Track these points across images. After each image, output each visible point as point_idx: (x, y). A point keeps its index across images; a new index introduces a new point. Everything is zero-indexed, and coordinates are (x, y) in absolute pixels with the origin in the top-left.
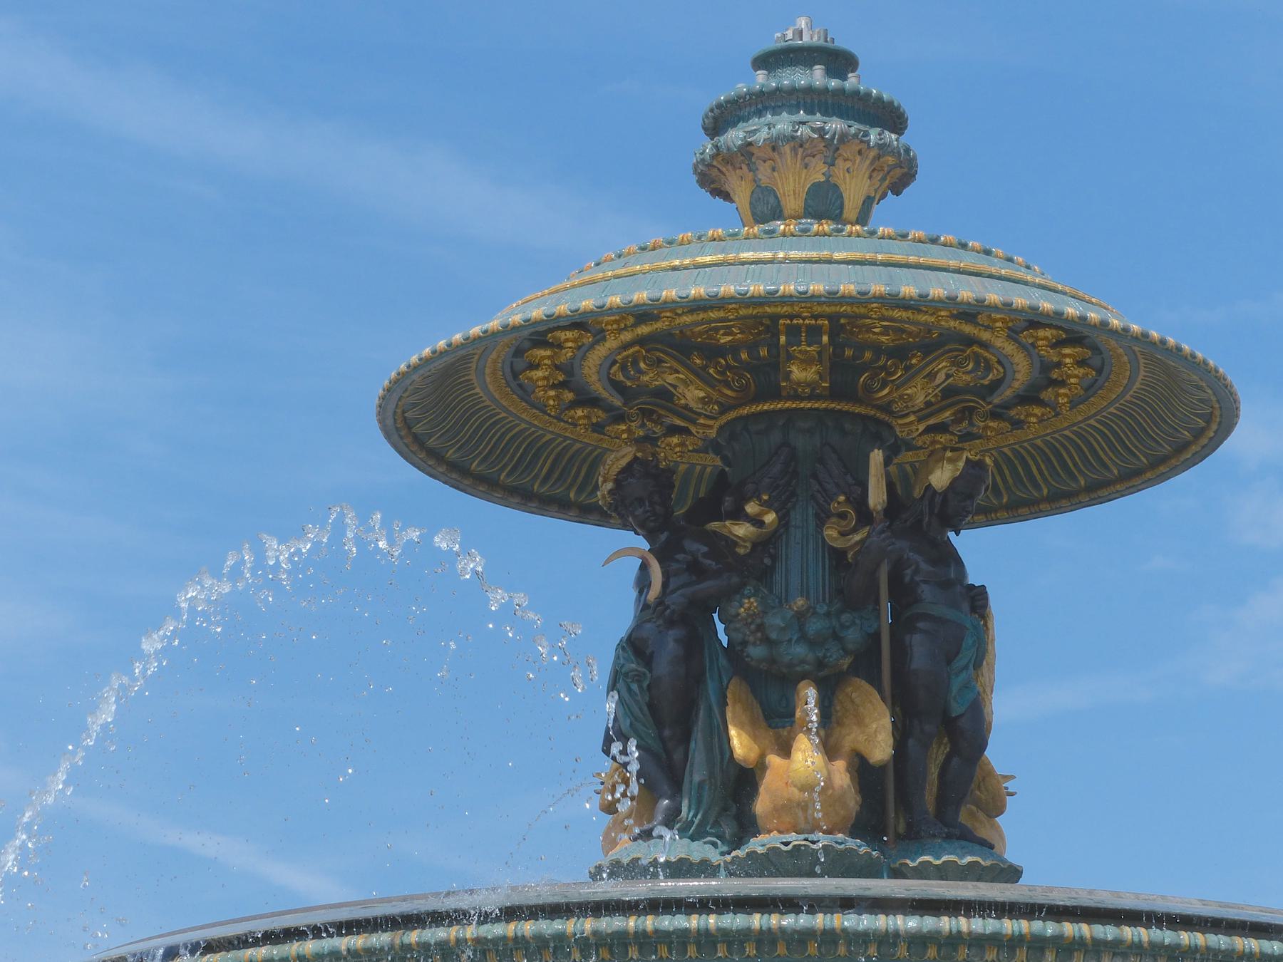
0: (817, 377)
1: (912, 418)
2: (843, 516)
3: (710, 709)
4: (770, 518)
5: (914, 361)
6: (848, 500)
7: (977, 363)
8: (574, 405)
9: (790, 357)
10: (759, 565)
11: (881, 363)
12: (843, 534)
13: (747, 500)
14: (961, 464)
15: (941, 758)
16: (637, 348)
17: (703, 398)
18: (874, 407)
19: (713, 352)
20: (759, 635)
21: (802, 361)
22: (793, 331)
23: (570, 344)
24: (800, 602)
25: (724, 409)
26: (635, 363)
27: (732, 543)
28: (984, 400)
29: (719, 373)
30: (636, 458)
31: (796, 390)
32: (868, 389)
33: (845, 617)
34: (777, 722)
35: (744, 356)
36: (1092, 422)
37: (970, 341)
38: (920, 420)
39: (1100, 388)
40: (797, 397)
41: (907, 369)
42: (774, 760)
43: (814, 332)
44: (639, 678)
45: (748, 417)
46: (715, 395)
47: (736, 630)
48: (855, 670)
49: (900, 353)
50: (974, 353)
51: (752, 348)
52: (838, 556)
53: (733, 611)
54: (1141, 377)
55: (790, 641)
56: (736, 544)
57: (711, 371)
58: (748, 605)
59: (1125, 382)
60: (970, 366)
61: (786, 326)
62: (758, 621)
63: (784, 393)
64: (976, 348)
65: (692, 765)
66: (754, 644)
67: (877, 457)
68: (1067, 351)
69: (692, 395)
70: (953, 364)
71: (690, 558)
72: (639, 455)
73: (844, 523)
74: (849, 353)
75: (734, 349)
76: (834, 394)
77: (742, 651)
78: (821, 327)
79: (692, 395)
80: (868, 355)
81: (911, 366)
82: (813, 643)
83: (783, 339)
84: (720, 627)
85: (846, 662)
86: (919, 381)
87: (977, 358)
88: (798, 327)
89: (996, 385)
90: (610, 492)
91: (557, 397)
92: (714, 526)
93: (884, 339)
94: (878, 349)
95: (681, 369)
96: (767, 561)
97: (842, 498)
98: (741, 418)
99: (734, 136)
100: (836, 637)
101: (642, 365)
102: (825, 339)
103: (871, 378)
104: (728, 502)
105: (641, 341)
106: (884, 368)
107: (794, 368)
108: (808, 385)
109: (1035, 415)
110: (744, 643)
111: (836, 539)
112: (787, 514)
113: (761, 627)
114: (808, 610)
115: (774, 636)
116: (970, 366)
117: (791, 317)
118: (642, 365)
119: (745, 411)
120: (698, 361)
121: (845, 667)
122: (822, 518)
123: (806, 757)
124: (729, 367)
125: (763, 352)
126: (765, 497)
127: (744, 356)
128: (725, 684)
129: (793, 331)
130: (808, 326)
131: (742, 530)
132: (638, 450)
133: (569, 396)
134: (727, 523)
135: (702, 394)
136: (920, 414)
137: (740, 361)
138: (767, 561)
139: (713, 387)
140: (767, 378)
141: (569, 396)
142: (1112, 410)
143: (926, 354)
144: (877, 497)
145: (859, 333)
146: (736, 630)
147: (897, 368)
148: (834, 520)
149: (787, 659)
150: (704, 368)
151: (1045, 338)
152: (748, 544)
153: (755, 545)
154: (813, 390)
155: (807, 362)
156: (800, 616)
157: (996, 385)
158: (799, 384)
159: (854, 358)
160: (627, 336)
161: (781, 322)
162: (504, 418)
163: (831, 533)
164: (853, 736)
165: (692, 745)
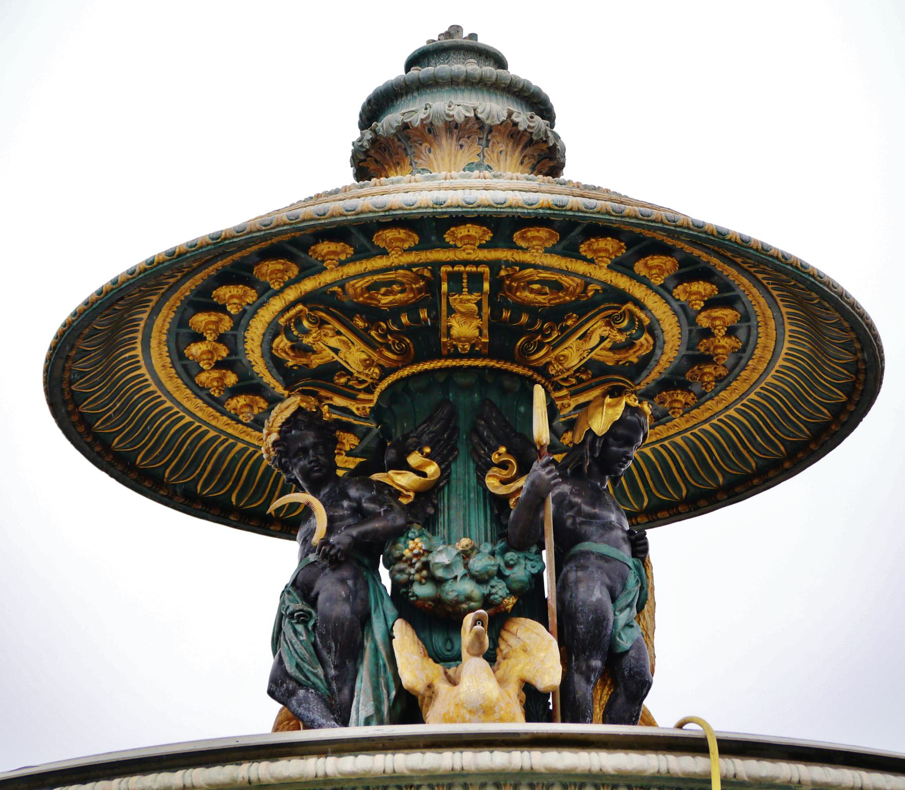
0: (477, 333)
1: (564, 392)
2: (503, 465)
3: (376, 650)
4: (432, 469)
5: (569, 323)
6: (508, 452)
7: (632, 321)
8: (234, 392)
9: (451, 311)
10: (425, 509)
11: (537, 327)
12: (504, 482)
13: (409, 453)
14: (620, 409)
15: (606, 698)
16: (300, 307)
17: (365, 360)
18: (530, 368)
19: (374, 315)
20: (424, 573)
21: (463, 314)
22: (454, 278)
23: (235, 301)
24: (465, 542)
25: (385, 372)
26: (298, 320)
27: (396, 494)
28: (632, 380)
29: (380, 336)
30: (300, 410)
31: (455, 347)
32: (525, 351)
33: (510, 556)
34: (447, 657)
35: (404, 319)
36: (732, 412)
37: (623, 297)
38: (573, 394)
39: (744, 369)
40: (456, 355)
41: (562, 330)
42: (443, 687)
43: (475, 280)
44: (304, 618)
45: (408, 377)
46: (375, 357)
47: (402, 571)
48: (520, 611)
49: (556, 315)
50: (630, 311)
51: (411, 308)
52: (498, 504)
53: (397, 553)
54: (785, 351)
55: (455, 578)
56: (398, 494)
57: (373, 333)
58: (413, 545)
59: (769, 357)
60: (625, 323)
61: (449, 274)
62: (423, 559)
63: (445, 352)
64: (630, 306)
65: (358, 702)
66: (421, 583)
67: (539, 393)
68: (718, 313)
69: (355, 356)
70: (608, 324)
71: (355, 504)
72: (303, 405)
73: (504, 472)
74: (506, 314)
75: (394, 312)
76: (493, 352)
77: (408, 592)
78: (481, 275)
79: (355, 356)
80: (524, 319)
81: (567, 327)
82: (480, 579)
83: (445, 287)
84: (384, 573)
85: (511, 601)
86: (573, 341)
87: (632, 315)
88: (460, 274)
89: (645, 362)
90: (275, 444)
91: (221, 379)
92: (376, 477)
93: (540, 298)
94: (532, 310)
95: (342, 330)
96: (431, 511)
97: (503, 450)
98: (402, 379)
99: (392, 119)
100: (500, 575)
101: (306, 324)
102: (486, 286)
103: (528, 341)
104: (391, 455)
105: (304, 299)
106: (541, 331)
107: (453, 322)
108: (468, 340)
109: (681, 402)
110: (410, 583)
111: (497, 487)
112: (448, 467)
113: (426, 565)
114: (473, 549)
115: (439, 573)
116: (625, 323)
117: (453, 263)
118: (306, 324)
119: (405, 372)
120: (361, 324)
121: (510, 607)
122: (483, 467)
123: (476, 678)
124: (389, 331)
125: (423, 314)
126: (428, 450)
127: (404, 319)
128: (390, 623)
129: (454, 278)
130: (470, 274)
131: (404, 480)
132: (302, 401)
133: (231, 379)
134: (391, 472)
135: (364, 356)
136: (572, 389)
137: (401, 325)
138: (431, 511)
139: (373, 348)
140: (427, 340)
141: (231, 379)
142: (752, 396)
143: (581, 316)
144: (541, 430)
145: (517, 289)
146: (402, 571)
147: (552, 330)
148: (495, 469)
149: (452, 596)
150: (366, 330)
151: (699, 293)
152: (412, 494)
153: (418, 494)
154: (473, 346)
155: (468, 315)
156: (465, 555)
157: (645, 362)
158: (459, 339)
159: (513, 319)
160: (291, 294)
161: (443, 269)
162: (170, 409)
163: (492, 483)
164: (520, 666)
165: (358, 684)
